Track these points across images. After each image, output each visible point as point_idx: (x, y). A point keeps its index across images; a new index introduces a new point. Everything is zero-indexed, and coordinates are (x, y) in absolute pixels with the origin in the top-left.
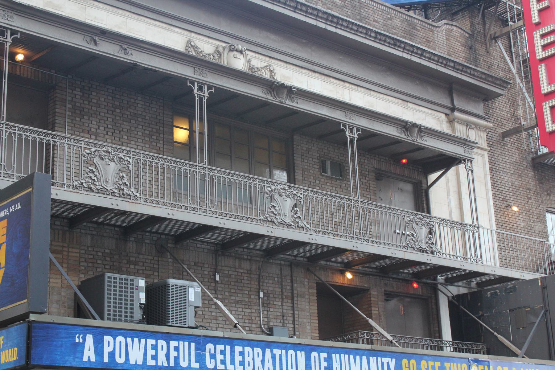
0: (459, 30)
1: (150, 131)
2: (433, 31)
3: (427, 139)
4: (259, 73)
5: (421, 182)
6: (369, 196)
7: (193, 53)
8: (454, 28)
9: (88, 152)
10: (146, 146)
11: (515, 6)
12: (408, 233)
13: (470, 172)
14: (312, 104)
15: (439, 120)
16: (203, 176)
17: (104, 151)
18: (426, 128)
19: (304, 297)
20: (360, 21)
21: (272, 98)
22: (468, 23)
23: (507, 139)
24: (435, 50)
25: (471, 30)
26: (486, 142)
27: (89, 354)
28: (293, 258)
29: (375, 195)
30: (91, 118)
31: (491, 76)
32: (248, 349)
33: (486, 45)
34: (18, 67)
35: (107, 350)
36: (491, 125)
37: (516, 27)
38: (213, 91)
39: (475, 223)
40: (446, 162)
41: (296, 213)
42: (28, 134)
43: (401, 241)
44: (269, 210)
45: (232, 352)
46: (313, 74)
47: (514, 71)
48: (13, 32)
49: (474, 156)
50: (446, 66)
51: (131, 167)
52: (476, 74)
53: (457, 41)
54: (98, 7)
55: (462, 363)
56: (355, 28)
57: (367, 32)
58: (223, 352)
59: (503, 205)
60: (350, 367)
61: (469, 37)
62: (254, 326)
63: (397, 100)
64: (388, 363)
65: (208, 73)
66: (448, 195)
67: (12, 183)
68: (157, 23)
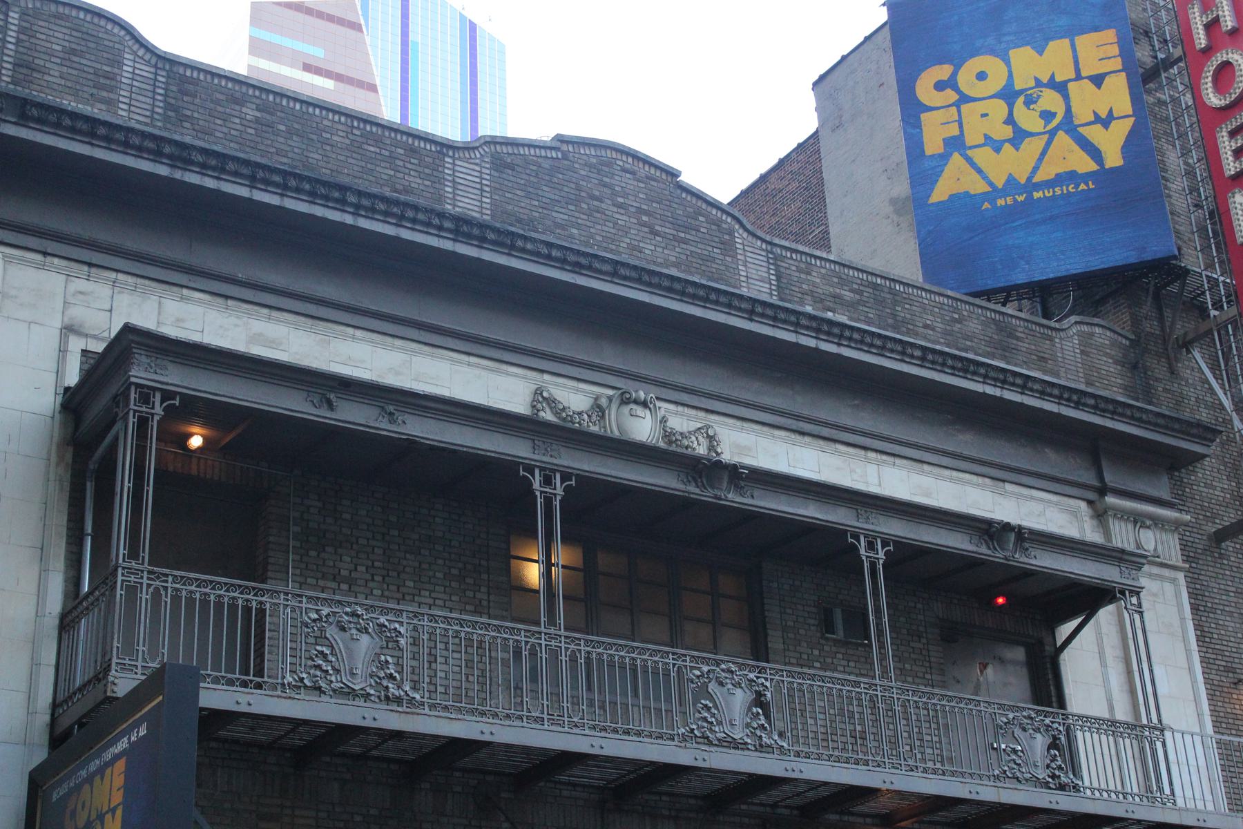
0: (1108, 333)
1: (460, 570)
2: (1051, 339)
3: (1038, 553)
4: (686, 442)
5: (1041, 643)
6: (928, 676)
7: (547, 415)
8: (1097, 330)
9: (315, 616)
10: (453, 598)
11: (1221, 279)
12: (1003, 746)
13: (1137, 617)
14: (783, 497)
15: (1074, 513)
16: (554, 654)
17: (347, 614)
18: (1032, 532)
20: (895, 328)
21: (697, 491)
22: (1126, 317)
23: (1228, 545)
24: (1057, 375)
25: (1134, 332)
26: (1179, 553)
28: (768, 809)
29: (942, 672)
30: (340, 551)
31: (1178, 420)
34: (194, 461)
37: (1224, 318)
38: (573, 483)
39: (1155, 720)
40: (1086, 599)
42: (193, 588)
43: (990, 767)
44: (697, 715)
46: (799, 438)
47: (1227, 403)
48: (167, 395)
49: (1144, 581)
50: (1078, 405)
51: (402, 641)
52: (1144, 417)
53: (1106, 354)
54: (353, 337)
56: (879, 343)
57: (903, 351)
59: (1226, 680)
61: (1131, 346)
63: (980, 480)
65: (562, 449)
66: (1103, 664)
67: (135, 683)
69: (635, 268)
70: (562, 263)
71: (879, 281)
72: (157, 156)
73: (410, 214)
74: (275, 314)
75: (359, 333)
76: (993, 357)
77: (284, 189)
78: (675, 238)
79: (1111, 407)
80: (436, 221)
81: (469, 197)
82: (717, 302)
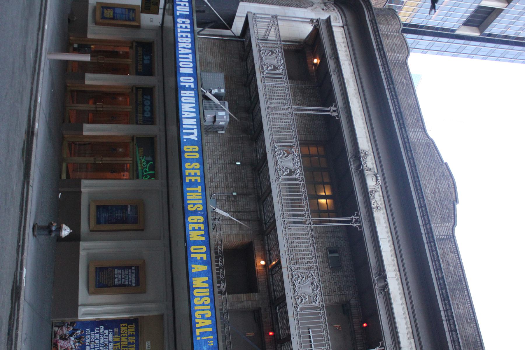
4: (372, 198)
19: (240, 230)
32: (190, 40)
41: (285, 170)
45: (187, 32)
46: (391, 242)
56: (436, 259)
58: (186, 28)
60: (188, 103)
62: (214, 189)
63: (410, 326)
64: (193, 134)
68: (367, 133)
69: (414, 163)
70: (404, 143)
71: (464, 283)
72: (378, 45)
73: (395, 100)
74: (356, 84)
75: (360, 103)
76: (462, 339)
77: (385, 72)
78: (436, 201)
80: (397, 107)
81: (413, 135)
82: (418, 194)
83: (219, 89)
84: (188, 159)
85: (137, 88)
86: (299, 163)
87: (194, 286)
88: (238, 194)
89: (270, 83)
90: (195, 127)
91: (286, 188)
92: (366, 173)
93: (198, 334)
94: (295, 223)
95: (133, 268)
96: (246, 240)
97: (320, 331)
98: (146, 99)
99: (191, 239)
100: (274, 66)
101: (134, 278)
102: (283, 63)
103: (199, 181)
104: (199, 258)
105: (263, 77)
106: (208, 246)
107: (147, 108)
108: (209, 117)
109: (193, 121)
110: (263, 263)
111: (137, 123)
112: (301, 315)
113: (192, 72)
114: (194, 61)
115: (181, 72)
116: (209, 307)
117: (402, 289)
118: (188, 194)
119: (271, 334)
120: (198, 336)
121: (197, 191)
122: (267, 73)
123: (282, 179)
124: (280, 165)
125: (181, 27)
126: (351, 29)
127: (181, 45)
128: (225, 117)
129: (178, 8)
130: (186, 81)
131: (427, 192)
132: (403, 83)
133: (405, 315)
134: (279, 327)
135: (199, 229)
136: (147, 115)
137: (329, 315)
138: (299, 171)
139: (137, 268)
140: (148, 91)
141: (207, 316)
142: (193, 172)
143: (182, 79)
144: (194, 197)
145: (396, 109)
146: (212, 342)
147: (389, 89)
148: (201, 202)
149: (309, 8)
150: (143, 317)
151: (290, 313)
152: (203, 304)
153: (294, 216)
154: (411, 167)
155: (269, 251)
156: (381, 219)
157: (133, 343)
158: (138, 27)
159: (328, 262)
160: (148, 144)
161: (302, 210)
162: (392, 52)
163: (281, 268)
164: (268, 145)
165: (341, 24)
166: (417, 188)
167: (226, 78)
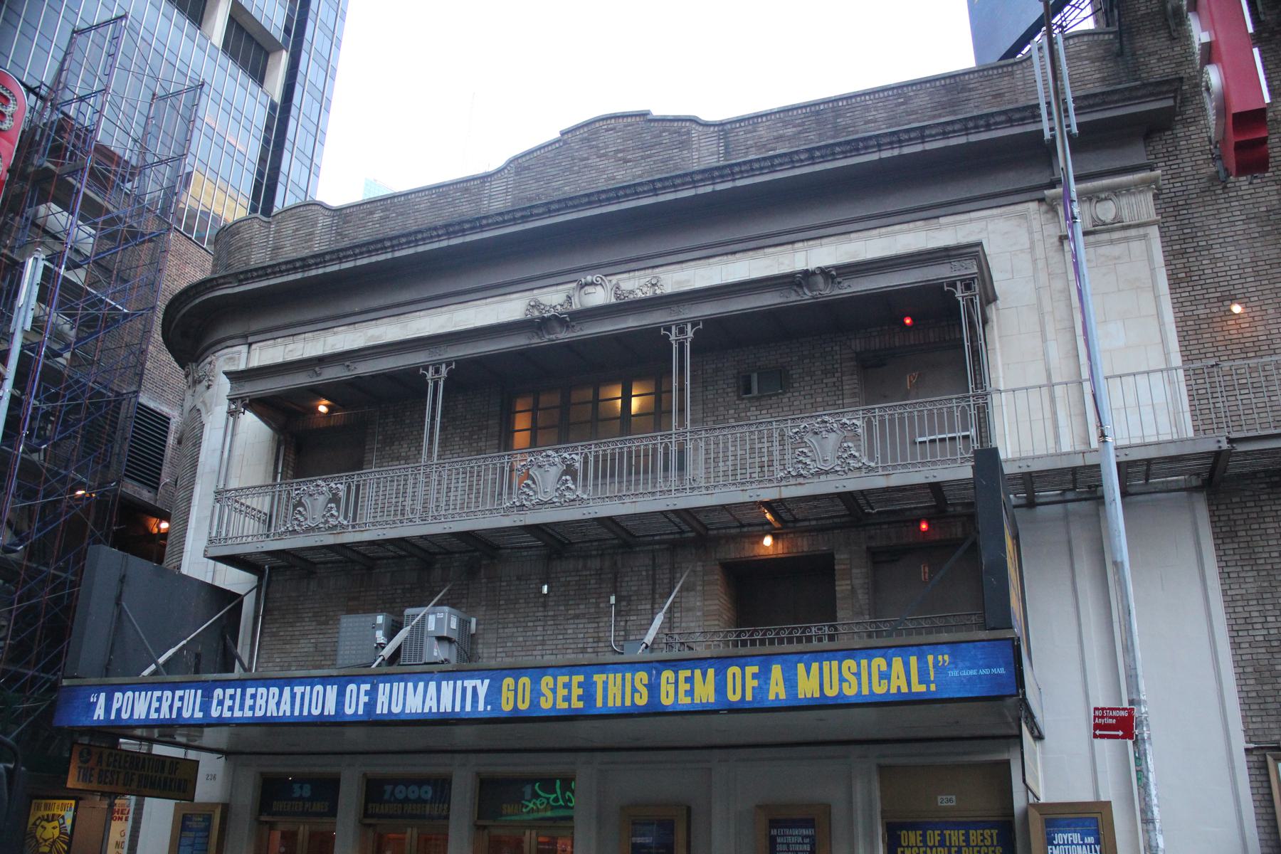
0: (1086, 39)
2: (1011, 74)
3: (846, 284)
15: (1023, 216)
18: (837, 268)
19: (693, 590)
27: (99, 713)
28: (677, 536)
32: (262, 690)
33: (1169, 27)
35: (115, 706)
36: (1159, 172)
45: (243, 695)
50: (988, 127)
53: (1081, 59)
55: (634, 672)
58: (232, 697)
60: (405, 699)
62: (601, 644)
63: (912, 225)
64: (475, 689)
69: (559, 201)
70: (514, 221)
72: (295, 270)
73: (420, 236)
74: (379, 322)
75: (422, 313)
76: (940, 116)
78: (643, 158)
79: (1027, 114)
81: (497, 202)
82: (626, 196)
83: (375, 627)
84: (531, 701)
85: (366, 814)
86: (550, 453)
87: (817, 695)
88: (615, 592)
89: (366, 515)
90: (459, 683)
91: (604, 484)
92: (576, 306)
93: (923, 688)
94: (681, 467)
95: (774, 832)
96: (717, 576)
97: (921, 418)
98: (392, 793)
99: (712, 700)
100: (330, 501)
101: (796, 832)
102: (325, 480)
103: (581, 678)
104: (755, 683)
105: (353, 527)
106: (729, 661)
107: (413, 793)
108: (438, 652)
109: (447, 687)
110: (768, 541)
111: (447, 817)
112: (884, 459)
113: (335, 687)
114: (310, 681)
115: (333, 713)
116: (864, 662)
117: (832, 239)
118: (610, 704)
119: (924, 526)
120: (928, 687)
121: (605, 683)
122: (345, 518)
123: (584, 492)
124: (552, 495)
125: (231, 709)
126: (255, 326)
127: (272, 711)
128: (440, 616)
129: (186, 714)
130: (355, 701)
131: (624, 176)
132: (381, 218)
133: (886, 235)
134: (910, 509)
135: (689, 680)
136: (427, 793)
137: (885, 398)
138: (566, 455)
139: (774, 823)
140: (374, 789)
141: (884, 668)
142: (562, 692)
143: (349, 711)
144: (618, 691)
145: (439, 236)
146: (940, 658)
147: (393, 248)
148: (628, 675)
149: (204, 418)
150: (883, 812)
151: (880, 482)
152: (858, 675)
153: (666, 469)
154: (567, 207)
155: (742, 526)
156: (677, 278)
157: (942, 835)
158: (226, 808)
159: (770, 396)
160: (495, 793)
161: (655, 450)
162: (311, 240)
163: (781, 501)
164: (506, 522)
165: (244, 348)
166: (613, 198)
167: (351, 611)
